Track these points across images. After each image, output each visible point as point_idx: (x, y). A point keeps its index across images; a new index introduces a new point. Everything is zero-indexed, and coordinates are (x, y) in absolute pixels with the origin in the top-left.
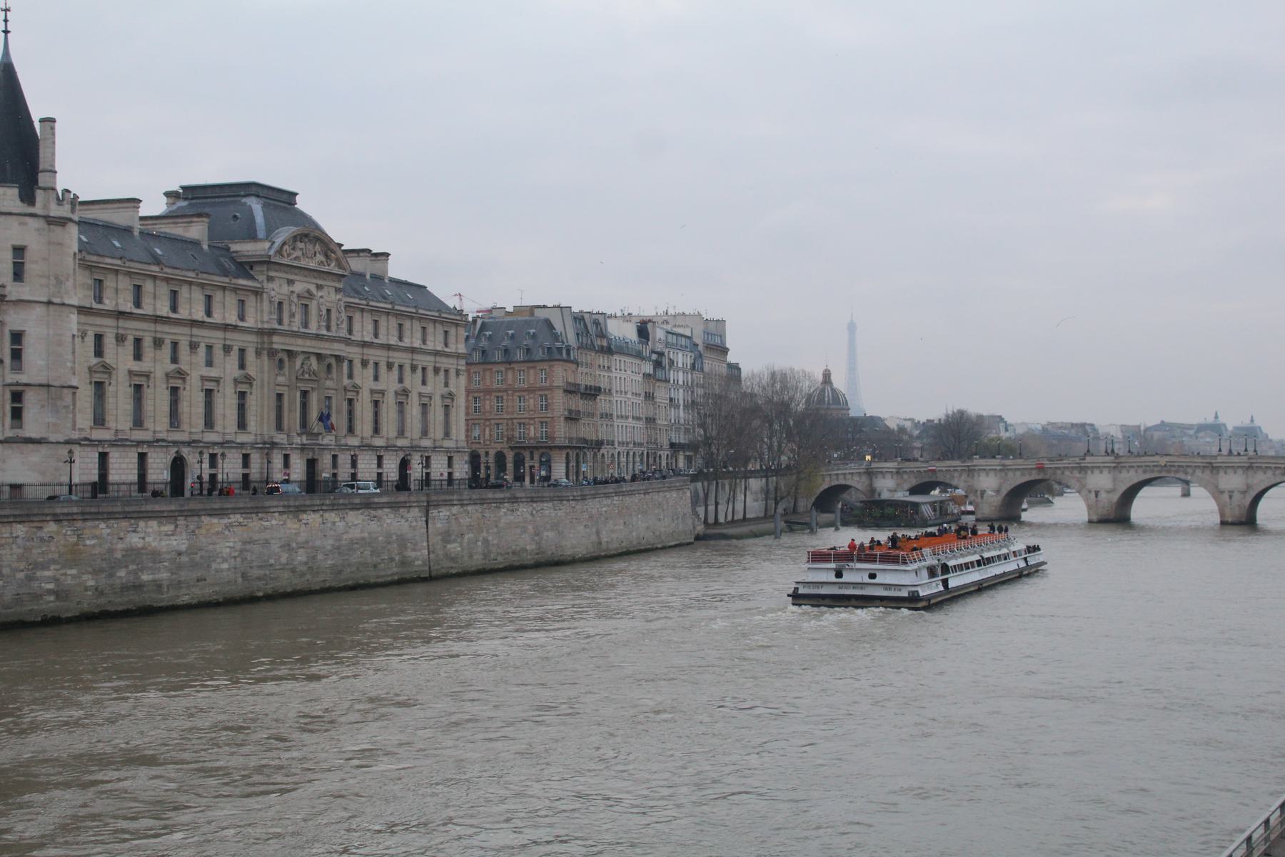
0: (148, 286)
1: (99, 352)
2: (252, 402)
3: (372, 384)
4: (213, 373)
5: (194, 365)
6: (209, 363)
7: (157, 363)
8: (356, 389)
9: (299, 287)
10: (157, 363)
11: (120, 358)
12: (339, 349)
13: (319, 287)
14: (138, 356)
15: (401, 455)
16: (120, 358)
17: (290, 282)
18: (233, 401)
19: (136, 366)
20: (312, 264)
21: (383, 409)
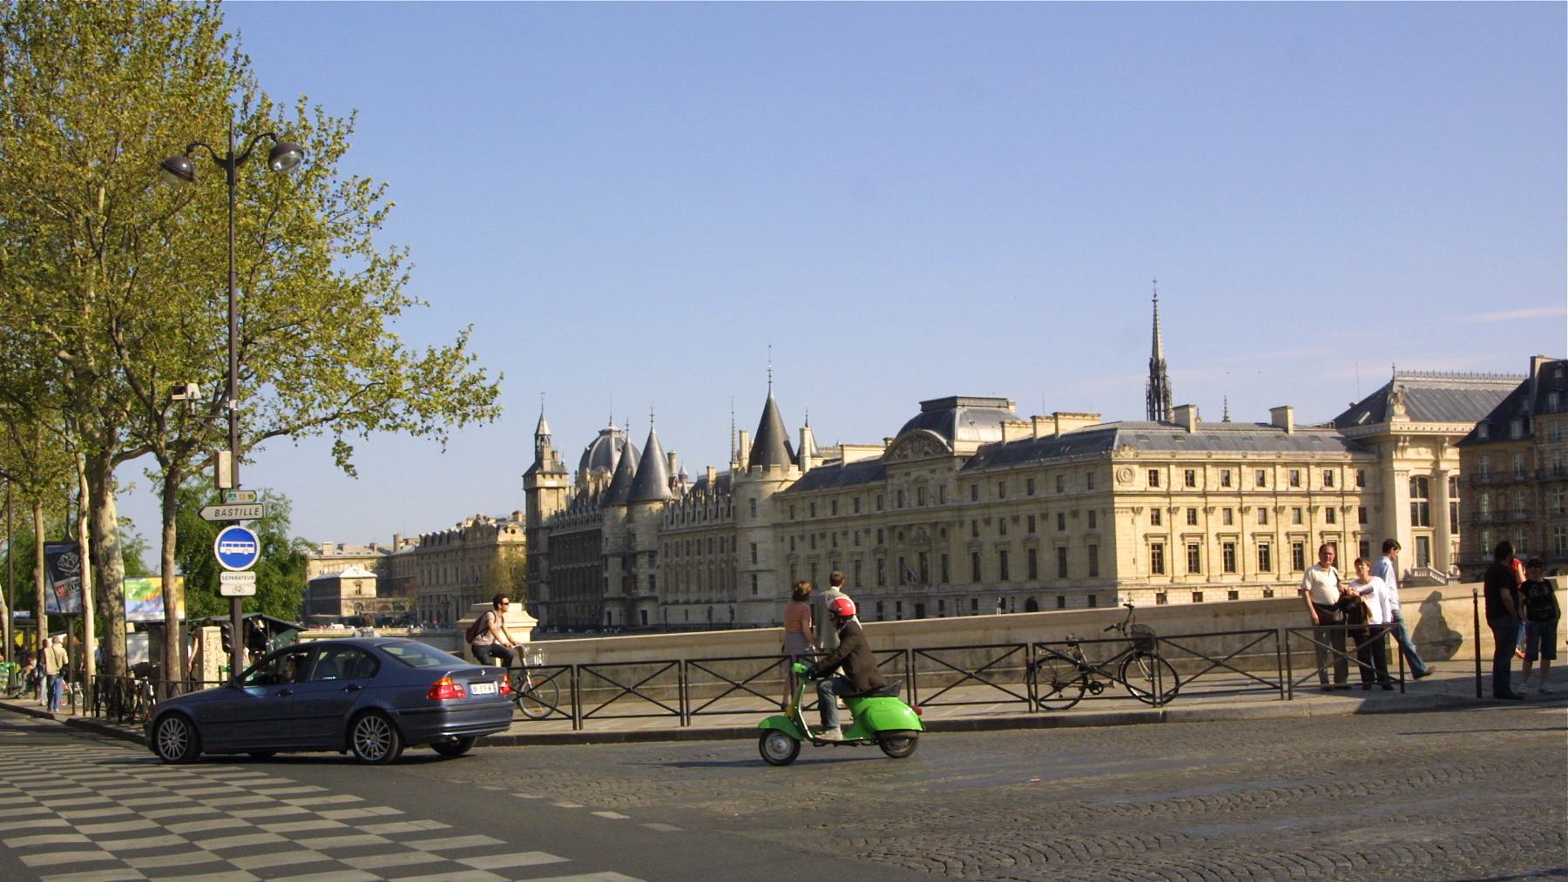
0: (819, 502)
1: (793, 548)
2: (887, 563)
3: (996, 537)
4: (859, 549)
5: (846, 547)
6: (857, 543)
7: (823, 548)
8: (981, 545)
9: (913, 476)
10: (823, 548)
11: (803, 549)
12: (909, 520)
13: (933, 471)
14: (813, 547)
15: (1026, 597)
16: (803, 549)
17: (908, 474)
18: (875, 565)
19: (811, 552)
20: (922, 457)
21: (1010, 557)
